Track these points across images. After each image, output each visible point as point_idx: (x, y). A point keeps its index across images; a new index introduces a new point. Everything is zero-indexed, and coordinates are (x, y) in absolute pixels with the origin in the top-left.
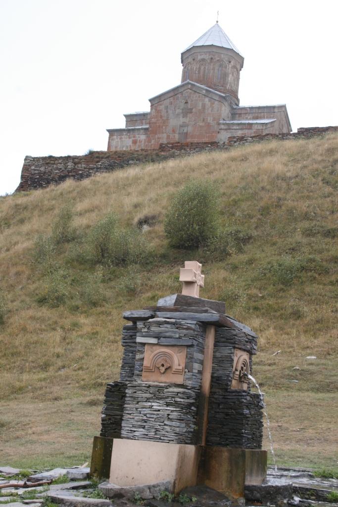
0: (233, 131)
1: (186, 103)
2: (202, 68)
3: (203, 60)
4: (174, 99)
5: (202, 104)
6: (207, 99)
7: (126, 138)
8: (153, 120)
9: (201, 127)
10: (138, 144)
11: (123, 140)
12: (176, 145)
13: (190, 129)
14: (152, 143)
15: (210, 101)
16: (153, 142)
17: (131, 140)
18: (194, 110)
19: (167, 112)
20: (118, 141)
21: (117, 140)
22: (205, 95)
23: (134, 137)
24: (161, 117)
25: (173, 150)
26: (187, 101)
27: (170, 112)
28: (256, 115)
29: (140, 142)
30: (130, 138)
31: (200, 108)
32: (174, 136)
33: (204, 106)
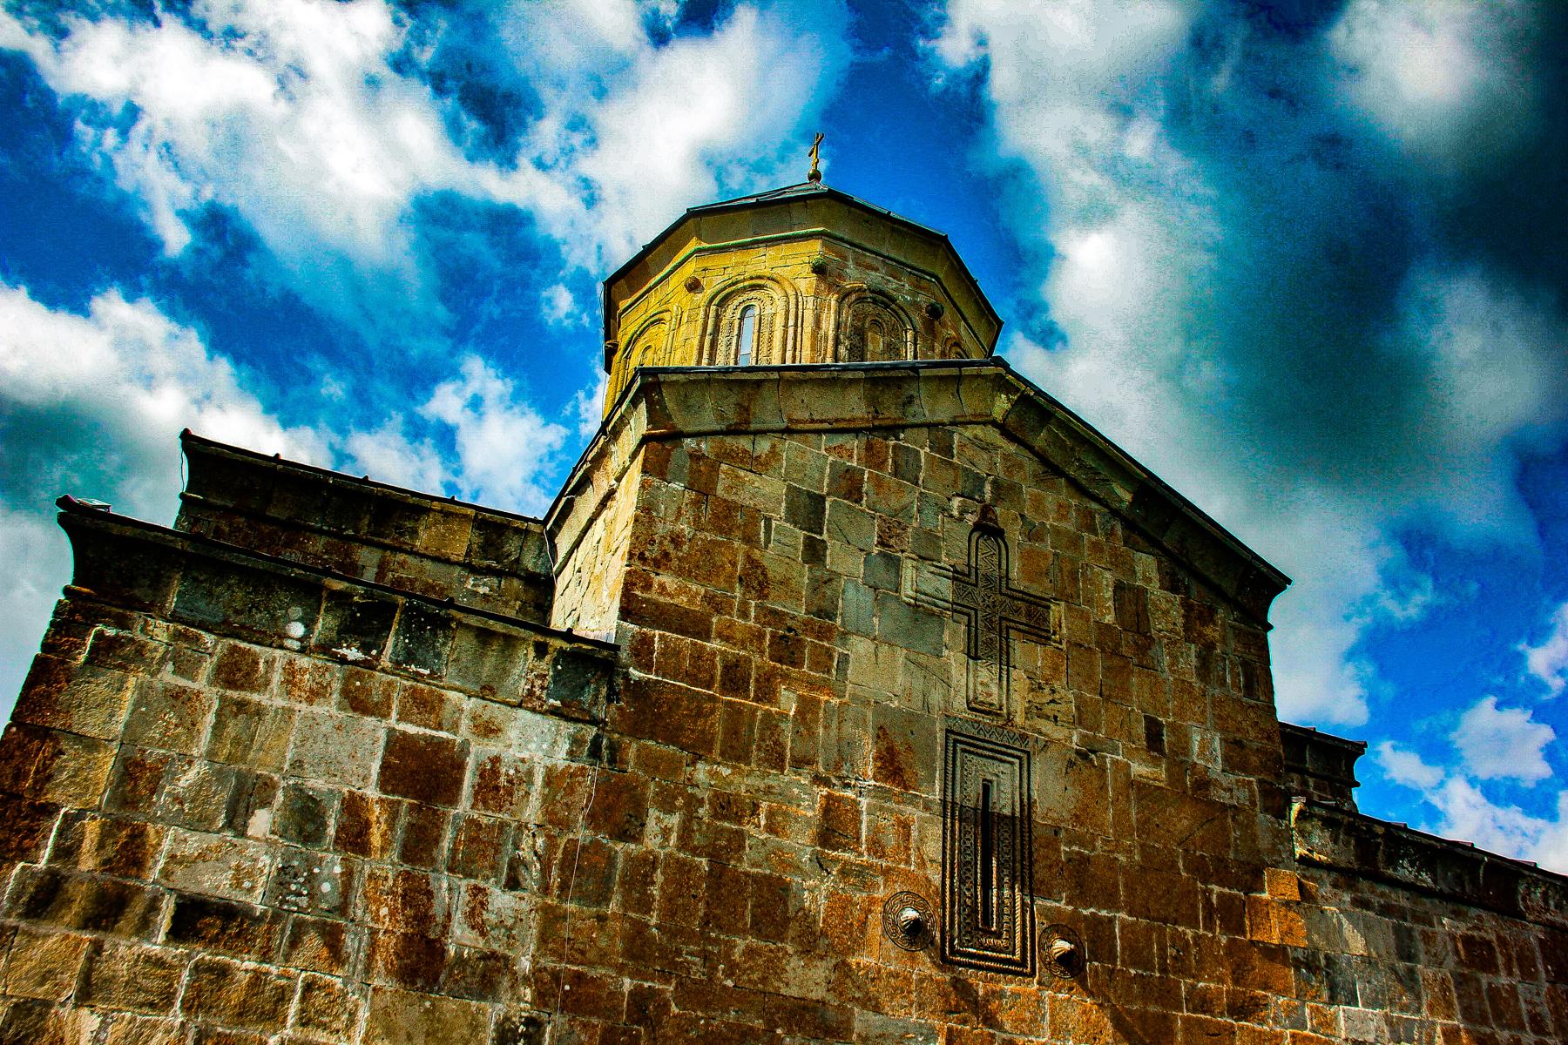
4: (873, 456)
7: (315, 695)
8: (667, 580)
9: (1141, 789)
10: (464, 805)
11: (272, 699)
14: (652, 842)
16: (660, 832)
17: (374, 732)
19: (814, 552)
20: (178, 697)
21: (168, 676)
23: (425, 705)
24: (756, 580)
27: (845, 561)
29: (492, 787)
30: (358, 703)
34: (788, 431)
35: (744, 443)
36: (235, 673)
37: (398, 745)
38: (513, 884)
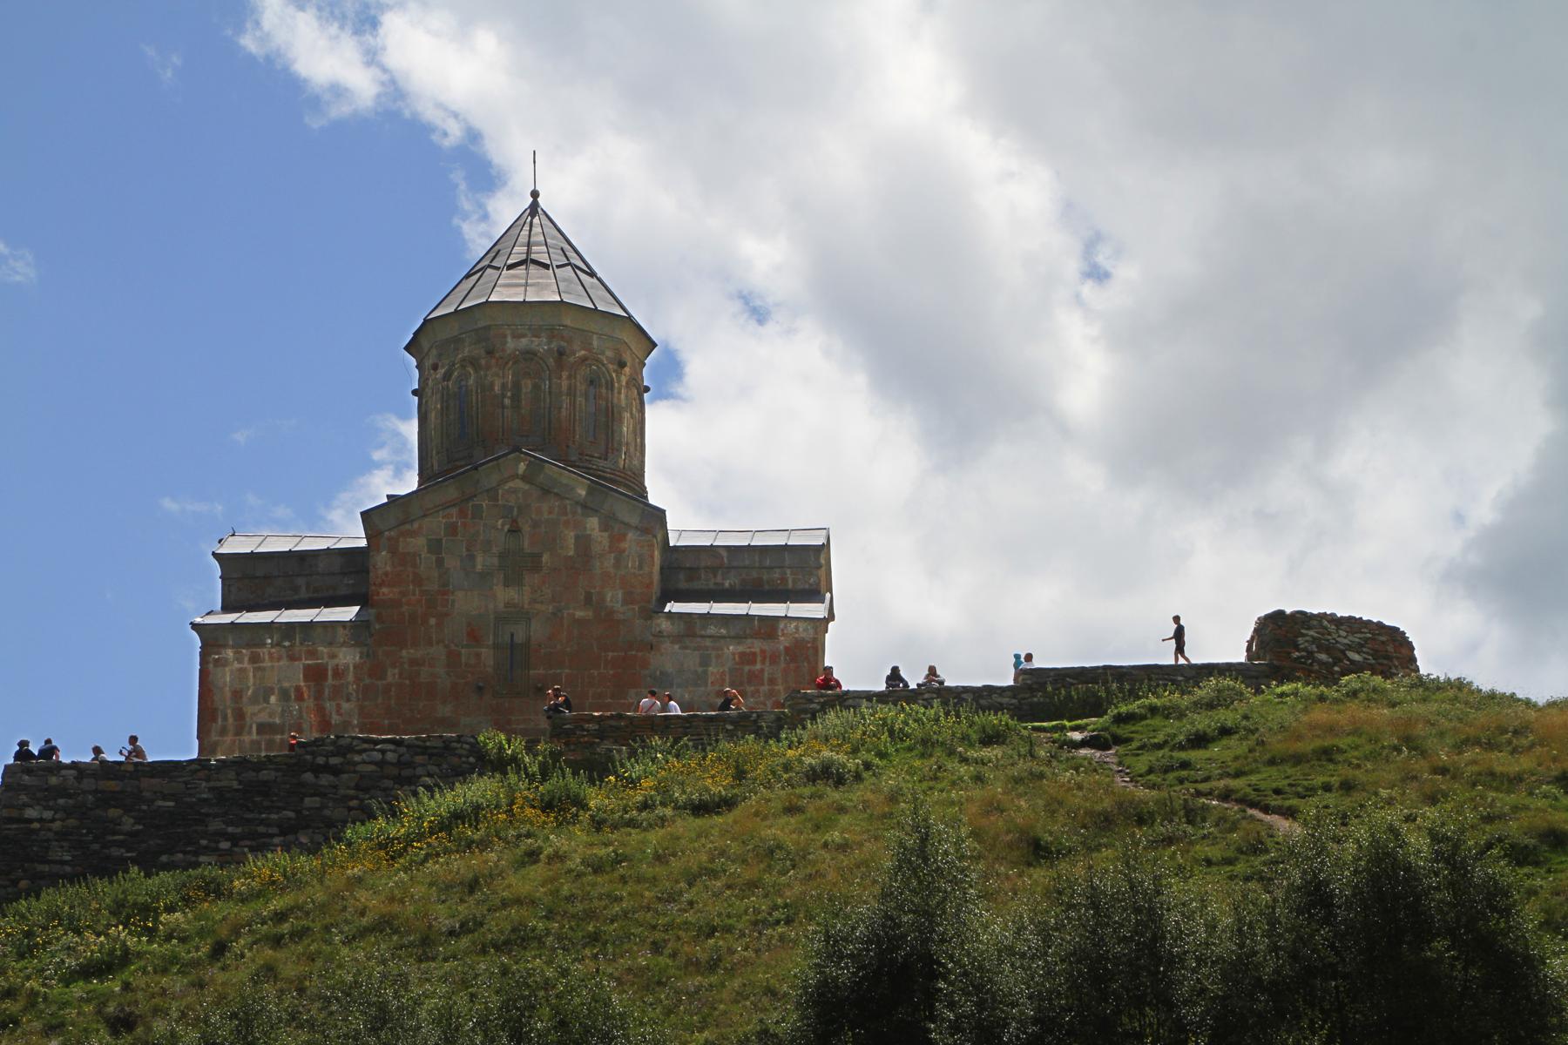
0: (708, 643)
1: (515, 531)
2: (527, 385)
3: (529, 355)
4: (462, 514)
5: (577, 538)
6: (593, 523)
7: (279, 659)
8: (385, 590)
9: (581, 622)
10: (330, 680)
11: (267, 664)
12: (613, 723)
13: (538, 631)
14: (390, 679)
15: (605, 527)
16: (392, 675)
17: (299, 666)
18: (545, 558)
19: (440, 562)
20: (241, 670)
21: (236, 665)
22: (585, 506)
23: (312, 654)
24: (418, 581)
25: (607, 745)
26: (514, 521)
27: (451, 563)
28: (755, 574)
29: (338, 673)
30: (292, 658)
31: (571, 553)
32: (478, 655)
33: (584, 542)
34: (425, 516)
35: (407, 527)
36: (255, 659)
37: (307, 668)
38: (348, 700)
